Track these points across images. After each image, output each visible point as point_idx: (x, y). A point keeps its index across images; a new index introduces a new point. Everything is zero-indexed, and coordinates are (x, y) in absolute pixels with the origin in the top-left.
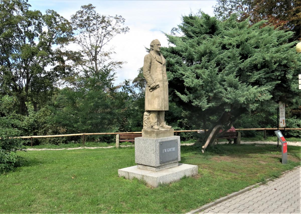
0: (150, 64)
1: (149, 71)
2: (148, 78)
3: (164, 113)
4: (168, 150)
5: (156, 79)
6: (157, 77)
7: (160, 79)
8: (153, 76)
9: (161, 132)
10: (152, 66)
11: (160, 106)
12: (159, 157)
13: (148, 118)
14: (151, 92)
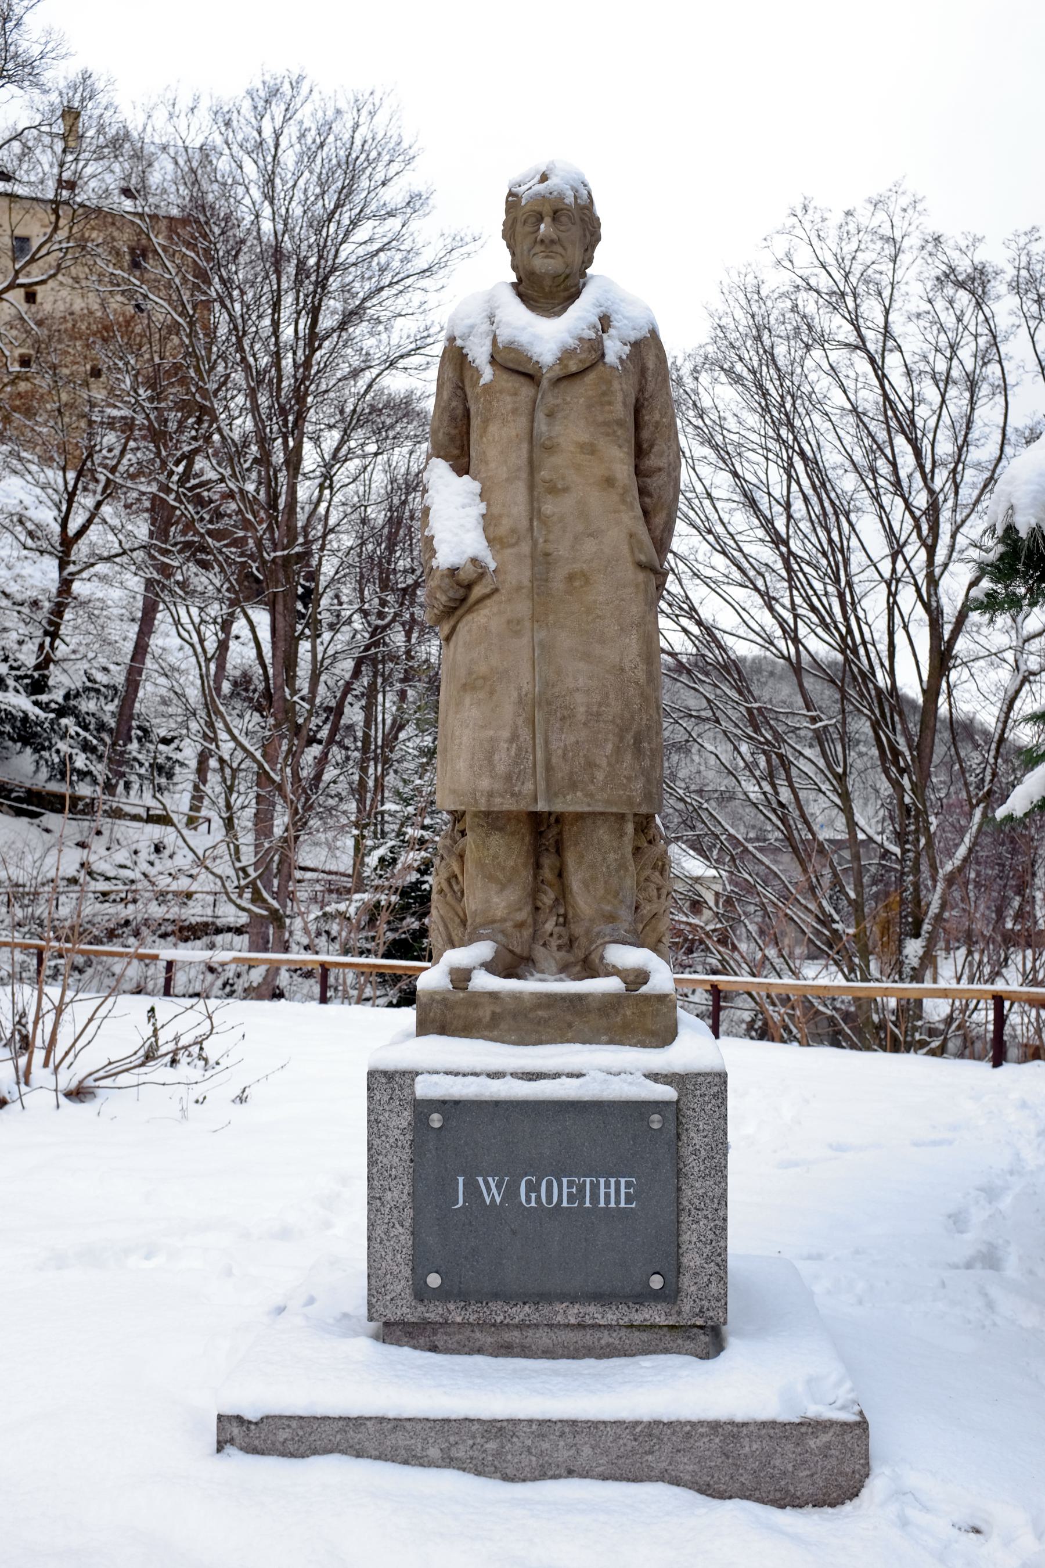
11: (501, 769)
12: (406, 1239)
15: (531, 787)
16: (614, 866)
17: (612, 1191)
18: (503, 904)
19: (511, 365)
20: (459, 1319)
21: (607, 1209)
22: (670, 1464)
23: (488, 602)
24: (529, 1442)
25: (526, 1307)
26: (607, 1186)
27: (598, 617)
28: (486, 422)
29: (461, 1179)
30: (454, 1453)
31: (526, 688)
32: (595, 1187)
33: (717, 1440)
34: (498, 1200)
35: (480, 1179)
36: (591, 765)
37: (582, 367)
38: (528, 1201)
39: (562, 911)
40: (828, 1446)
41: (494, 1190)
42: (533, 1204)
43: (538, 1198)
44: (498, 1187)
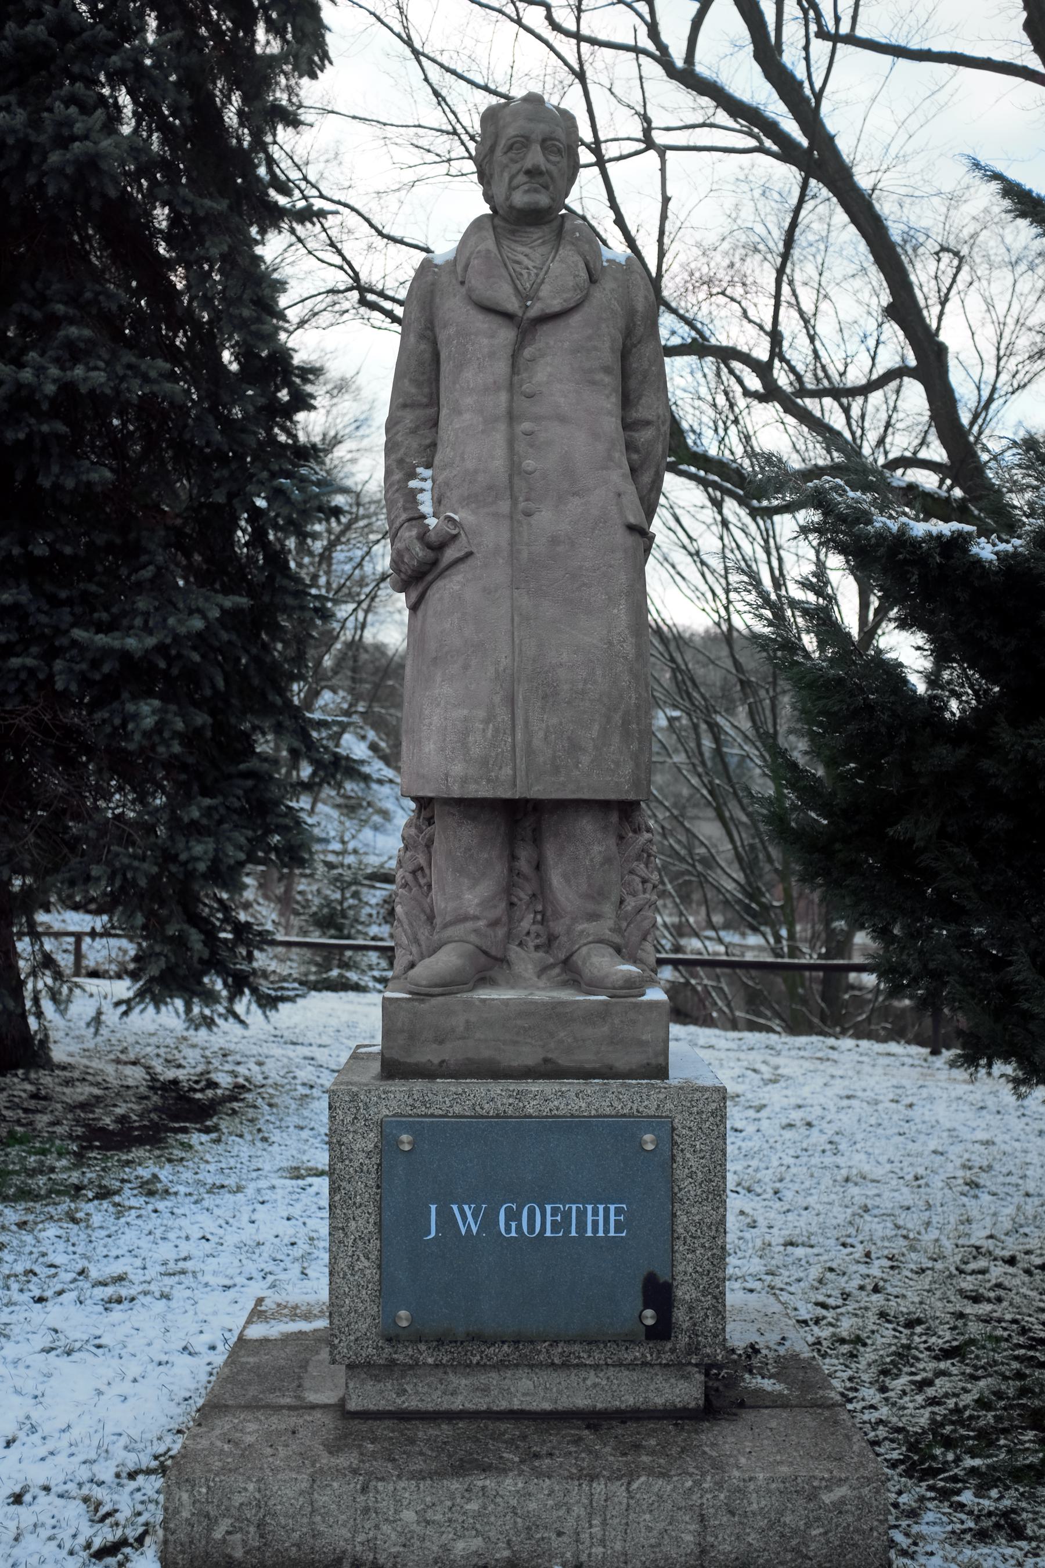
4: (513, 1216)
11: (476, 751)
12: (372, 1273)
15: (510, 772)
16: (598, 859)
17: (601, 1218)
18: (476, 901)
19: (488, 304)
20: (430, 1361)
21: (595, 1239)
22: (670, 1524)
23: (462, 567)
25: (505, 1347)
26: (595, 1213)
27: (584, 584)
28: (460, 367)
29: (433, 1207)
30: (429, 1515)
31: (504, 662)
32: (582, 1215)
33: (722, 1496)
34: (474, 1230)
35: (455, 1207)
36: (574, 747)
37: (566, 305)
38: (508, 1229)
39: (540, 908)
40: (843, 1501)
41: (470, 1219)
42: (513, 1234)
43: (519, 1228)
44: (475, 1216)
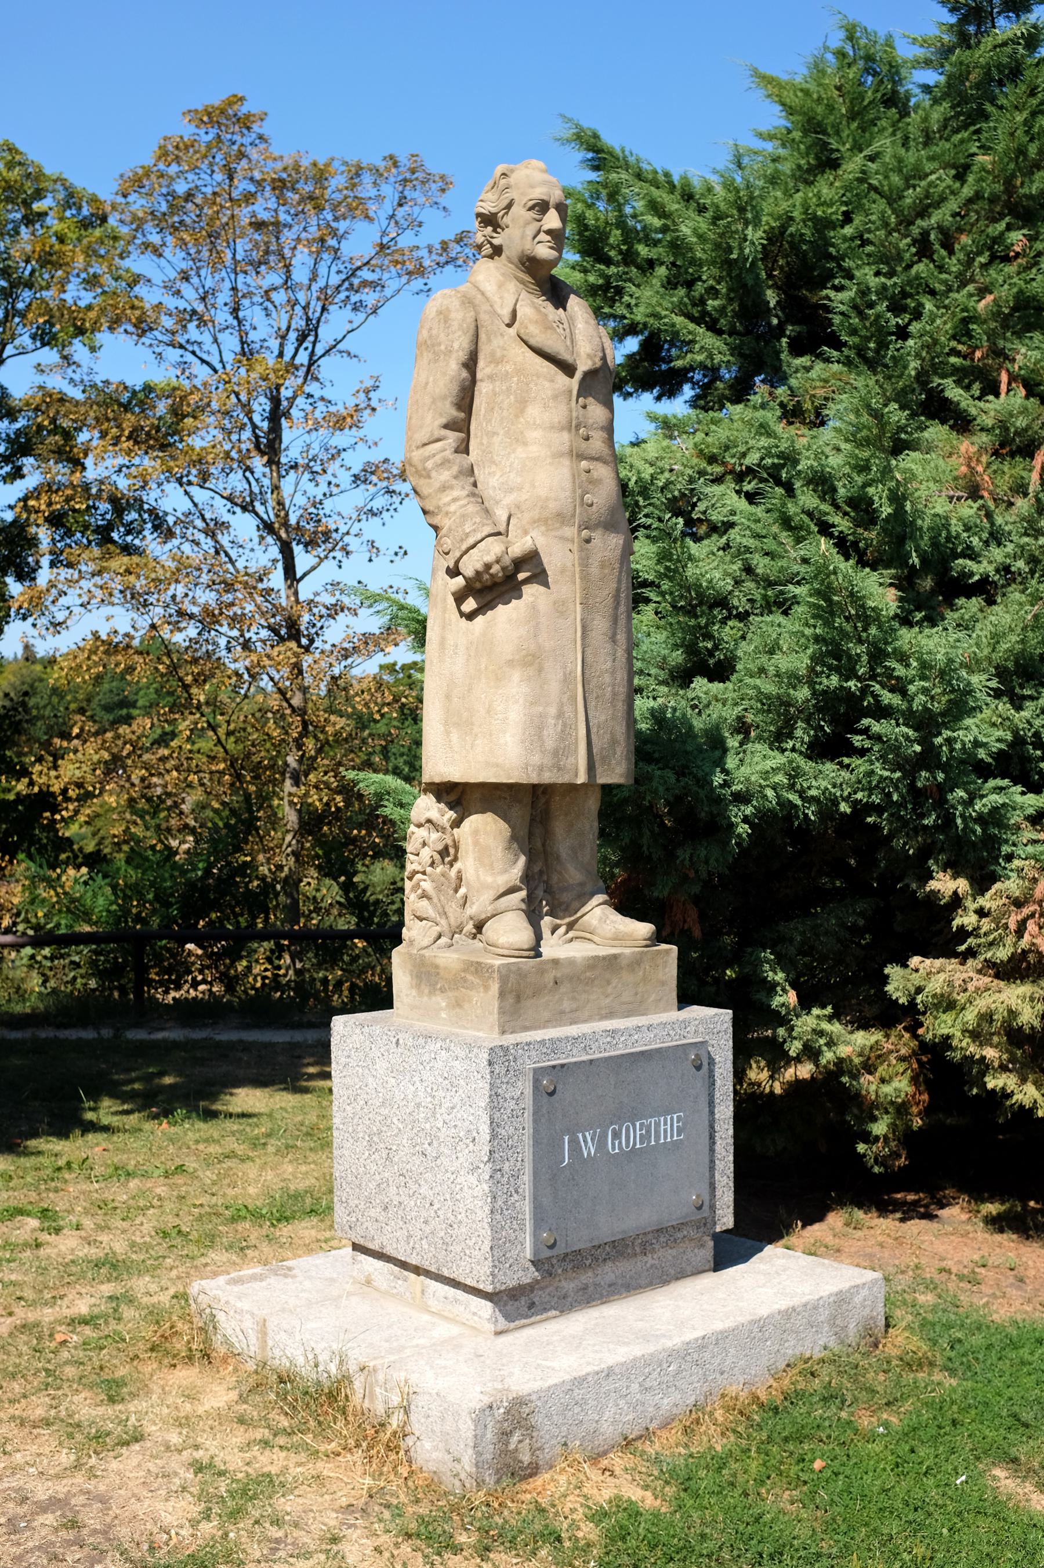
0: (465, 374)
1: (453, 438)
2: (446, 498)
3: (593, 804)
4: (616, 1135)
5: (509, 499)
6: (520, 489)
7: (553, 506)
8: (490, 480)
9: (549, 977)
10: (483, 391)
11: (550, 744)
13: (444, 852)
14: (470, 616)
24: (695, 1356)
26: (665, 1124)
29: (566, 1138)
30: (648, 1384)
32: (657, 1125)
38: (613, 1148)
